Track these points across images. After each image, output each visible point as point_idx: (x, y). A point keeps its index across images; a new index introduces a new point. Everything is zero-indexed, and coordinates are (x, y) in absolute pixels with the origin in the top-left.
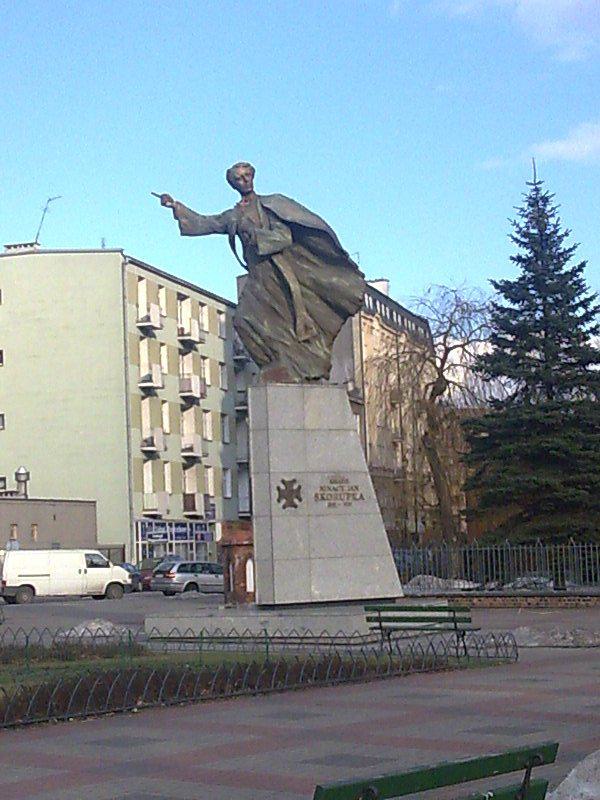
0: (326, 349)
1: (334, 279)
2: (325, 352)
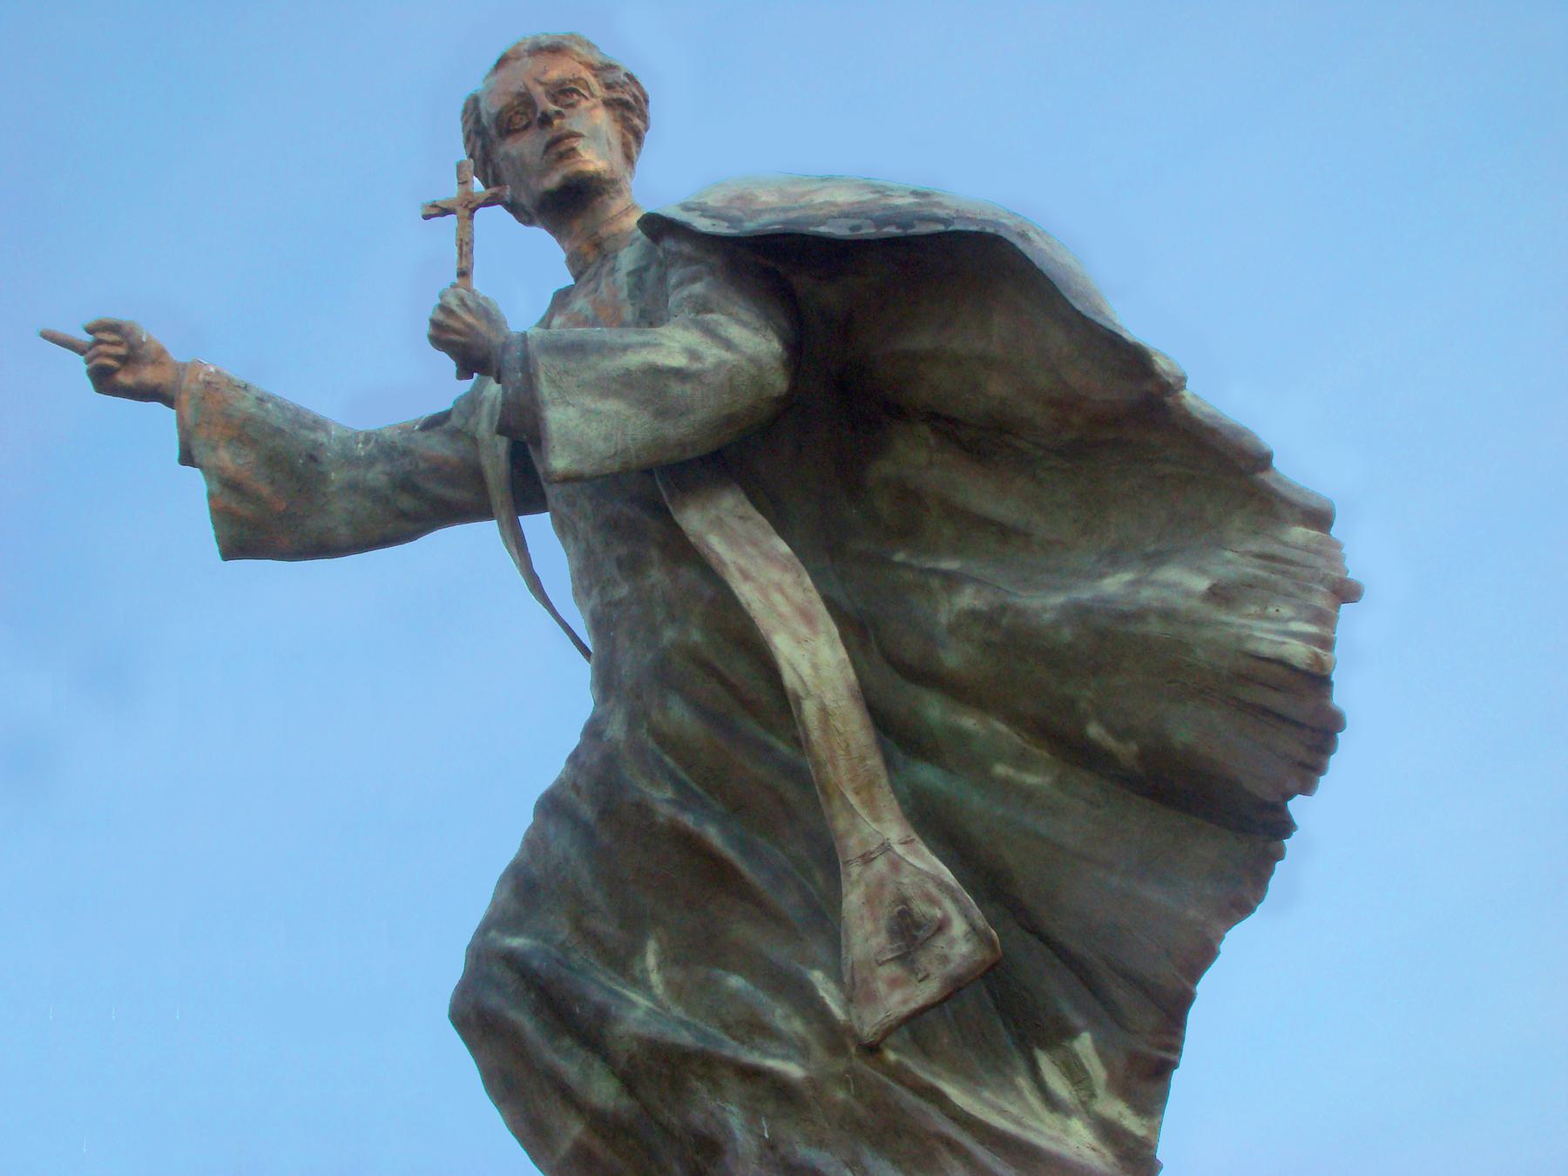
0: (1115, 1109)
1: (1114, 584)
2: (1109, 1132)
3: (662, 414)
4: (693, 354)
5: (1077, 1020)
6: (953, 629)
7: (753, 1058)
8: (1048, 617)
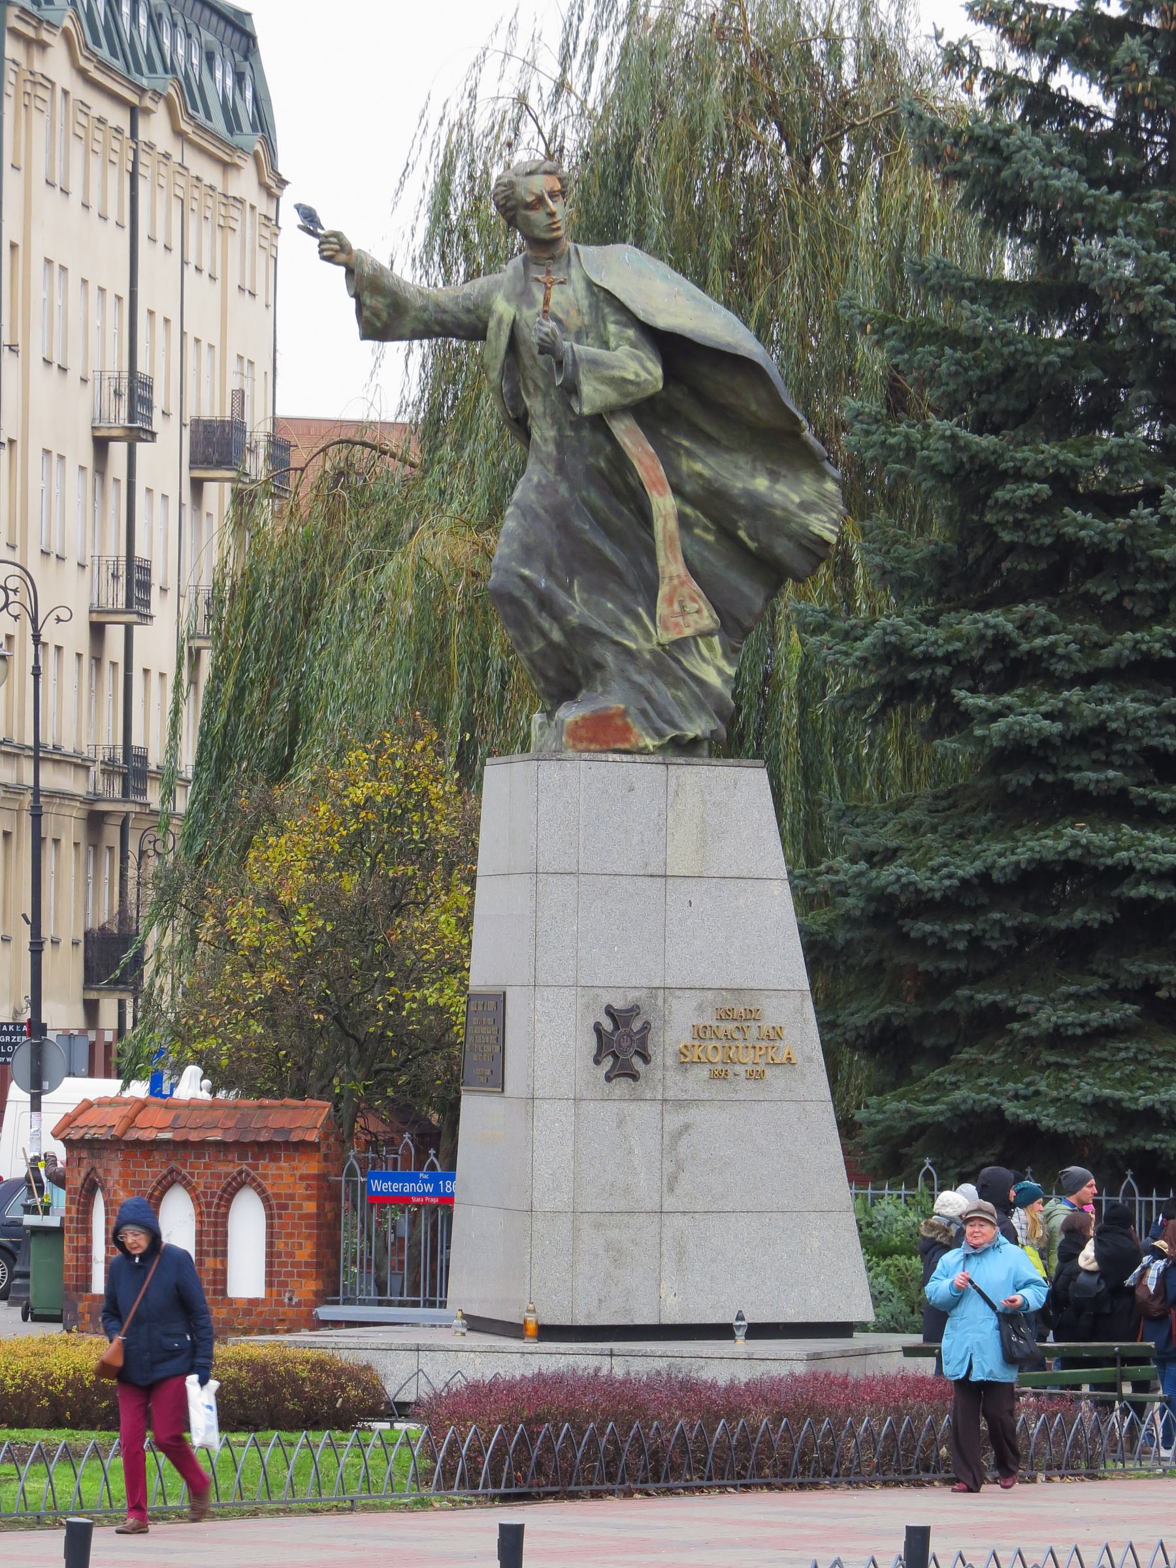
1: (761, 484)
4: (637, 375)
7: (618, 638)
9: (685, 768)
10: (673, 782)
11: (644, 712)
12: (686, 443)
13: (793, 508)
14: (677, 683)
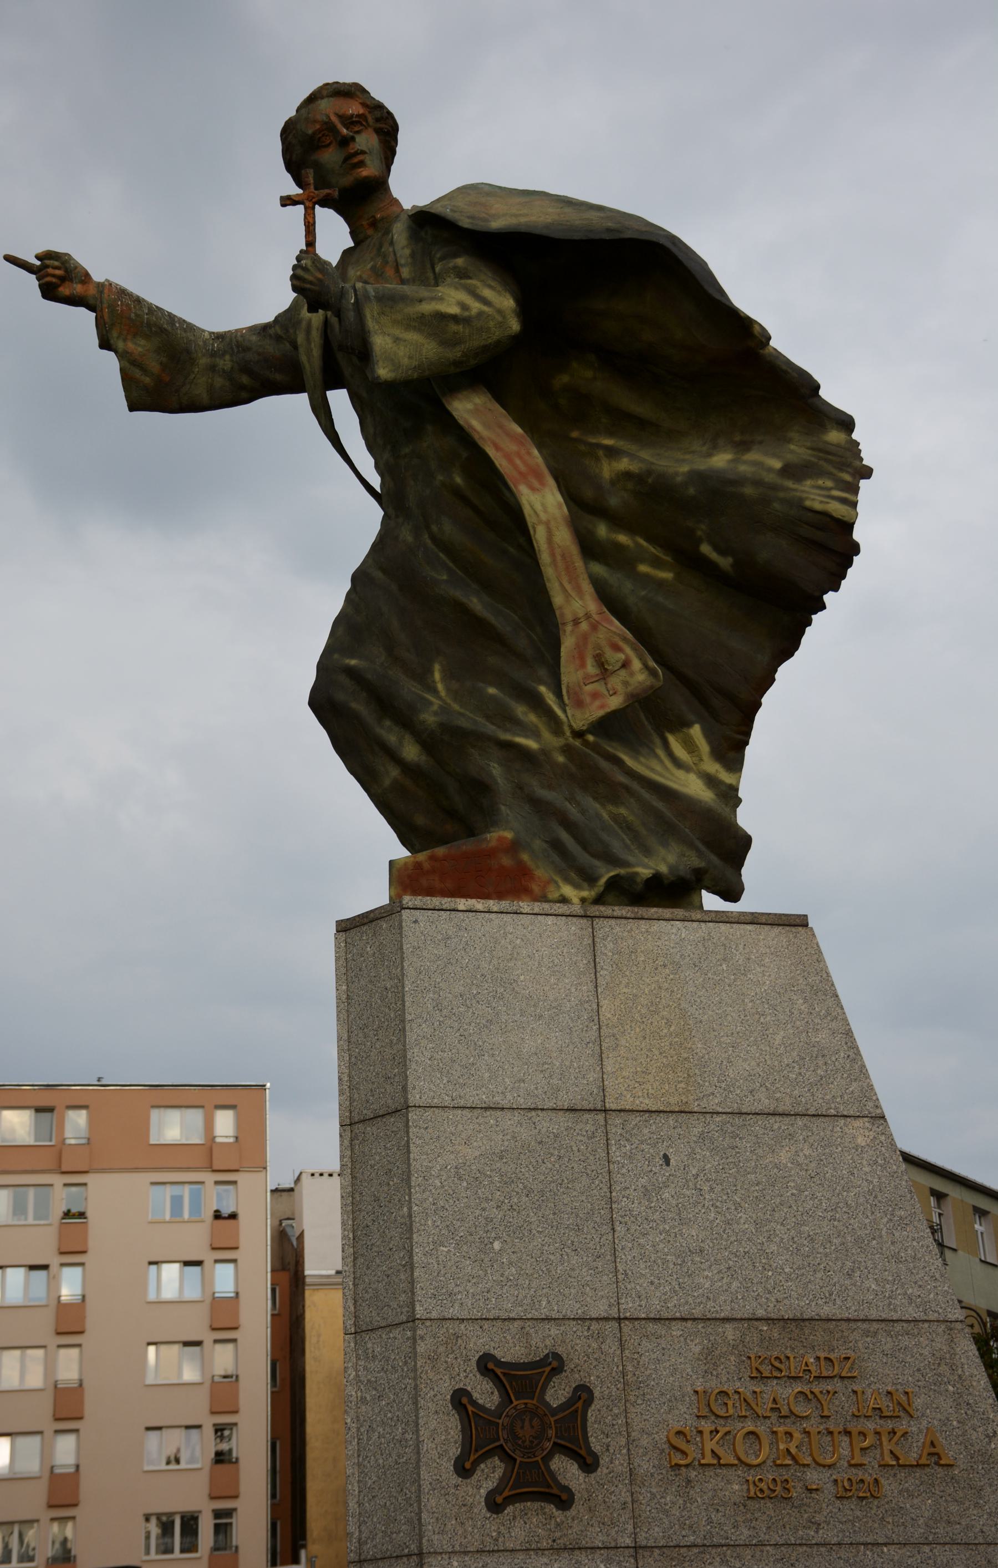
0: (713, 767)
1: (721, 460)
2: (711, 781)
3: (444, 343)
4: (464, 307)
5: (691, 717)
6: (613, 483)
8: (679, 479)
9: (631, 924)
10: (606, 949)
11: (557, 845)
12: (608, 442)
13: (770, 478)
14: (613, 793)
